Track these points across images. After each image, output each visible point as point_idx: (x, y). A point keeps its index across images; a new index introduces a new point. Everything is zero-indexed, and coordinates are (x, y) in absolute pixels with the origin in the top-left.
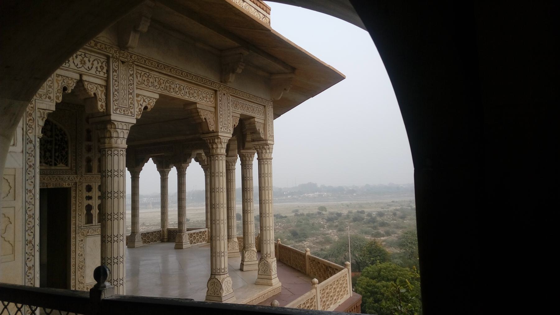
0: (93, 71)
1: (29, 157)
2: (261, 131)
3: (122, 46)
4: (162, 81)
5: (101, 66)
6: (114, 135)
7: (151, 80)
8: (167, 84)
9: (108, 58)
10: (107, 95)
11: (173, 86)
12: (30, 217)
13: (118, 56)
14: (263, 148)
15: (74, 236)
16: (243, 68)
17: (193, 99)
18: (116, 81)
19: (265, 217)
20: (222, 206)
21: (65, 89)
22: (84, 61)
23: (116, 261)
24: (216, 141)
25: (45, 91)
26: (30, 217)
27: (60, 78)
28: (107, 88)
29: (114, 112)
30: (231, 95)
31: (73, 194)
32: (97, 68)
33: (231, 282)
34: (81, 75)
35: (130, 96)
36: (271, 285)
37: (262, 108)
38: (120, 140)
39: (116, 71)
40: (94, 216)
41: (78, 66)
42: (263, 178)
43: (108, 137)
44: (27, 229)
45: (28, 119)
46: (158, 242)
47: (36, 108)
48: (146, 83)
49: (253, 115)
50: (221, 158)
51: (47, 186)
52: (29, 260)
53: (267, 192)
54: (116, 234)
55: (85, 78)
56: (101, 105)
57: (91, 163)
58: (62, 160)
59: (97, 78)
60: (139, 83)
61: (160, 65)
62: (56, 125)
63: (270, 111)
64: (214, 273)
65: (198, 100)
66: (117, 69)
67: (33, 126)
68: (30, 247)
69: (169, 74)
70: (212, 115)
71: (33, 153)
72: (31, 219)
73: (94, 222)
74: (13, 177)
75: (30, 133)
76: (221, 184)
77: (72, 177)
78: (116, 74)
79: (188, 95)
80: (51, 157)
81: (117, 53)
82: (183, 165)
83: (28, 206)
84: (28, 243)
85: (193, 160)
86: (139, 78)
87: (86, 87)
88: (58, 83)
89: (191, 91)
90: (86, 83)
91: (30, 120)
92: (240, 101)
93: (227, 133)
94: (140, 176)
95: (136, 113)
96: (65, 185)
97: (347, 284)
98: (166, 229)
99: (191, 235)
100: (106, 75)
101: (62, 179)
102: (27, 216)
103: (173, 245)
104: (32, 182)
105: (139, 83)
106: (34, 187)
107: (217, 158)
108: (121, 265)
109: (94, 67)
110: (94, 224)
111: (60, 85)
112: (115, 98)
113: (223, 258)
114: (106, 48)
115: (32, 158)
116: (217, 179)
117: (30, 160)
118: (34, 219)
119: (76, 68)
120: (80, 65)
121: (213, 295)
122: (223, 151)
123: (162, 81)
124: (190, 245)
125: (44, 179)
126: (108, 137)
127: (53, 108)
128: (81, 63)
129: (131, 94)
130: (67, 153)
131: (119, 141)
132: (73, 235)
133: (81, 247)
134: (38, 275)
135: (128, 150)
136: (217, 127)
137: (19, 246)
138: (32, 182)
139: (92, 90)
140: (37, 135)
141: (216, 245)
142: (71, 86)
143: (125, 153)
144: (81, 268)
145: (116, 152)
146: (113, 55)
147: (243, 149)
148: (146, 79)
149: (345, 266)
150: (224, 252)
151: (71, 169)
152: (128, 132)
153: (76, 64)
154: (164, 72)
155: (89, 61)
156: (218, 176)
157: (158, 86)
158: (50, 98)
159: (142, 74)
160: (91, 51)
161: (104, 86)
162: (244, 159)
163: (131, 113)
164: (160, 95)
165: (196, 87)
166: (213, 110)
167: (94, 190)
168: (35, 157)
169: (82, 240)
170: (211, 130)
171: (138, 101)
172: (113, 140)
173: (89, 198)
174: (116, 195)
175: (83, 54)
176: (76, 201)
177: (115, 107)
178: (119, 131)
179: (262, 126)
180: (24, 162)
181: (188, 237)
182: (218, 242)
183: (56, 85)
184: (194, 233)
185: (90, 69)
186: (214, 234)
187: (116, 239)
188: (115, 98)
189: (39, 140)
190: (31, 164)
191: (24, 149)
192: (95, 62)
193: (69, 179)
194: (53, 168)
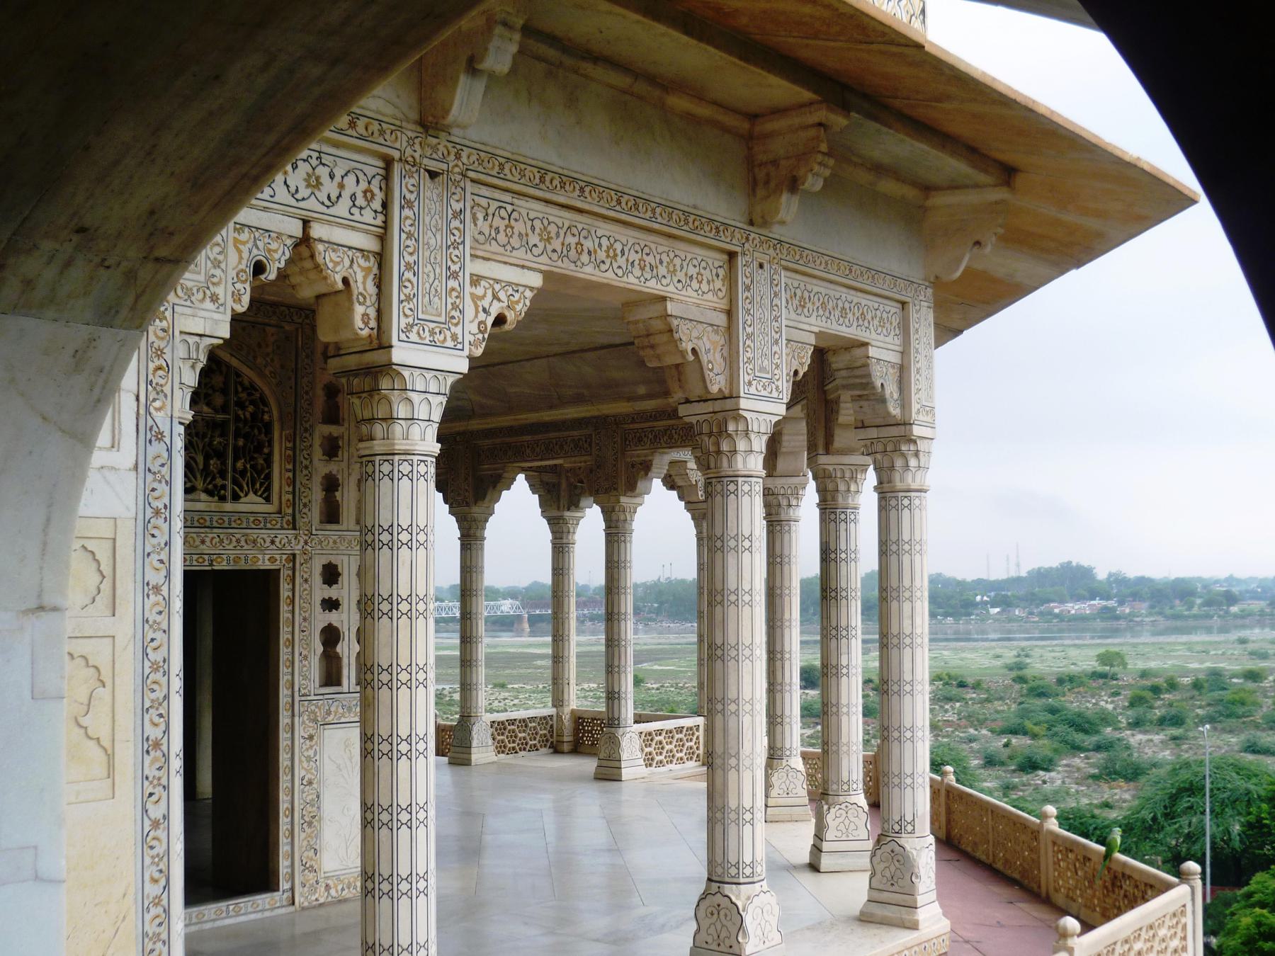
0: (342, 208)
1: (155, 485)
2: (891, 390)
3: (430, 122)
4: (553, 229)
5: (365, 192)
6: (401, 411)
7: (519, 227)
8: (572, 240)
9: (388, 163)
10: (381, 283)
11: (588, 244)
12: (155, 667)
13: (417, 155)
14: (897, 450)
15: (288, 721)
16: (827, 173)
17: (653, 287)
18: (410, 236)
19: (899, 693)
20: (747, 653)
21: (259, 268)
22: (318, 178)
23: (404, 817)
24: (731, 427)
25: (202, 278)
26: (155, 667)
27: (245, 236)
28: (382, 258)
29: (403, 337)
30: (786, 269)
31: (285, 591)
32: (353, 197)
33: (776, 909)
34: (306, 223)
35: (452, 283)
36: (914, 926)
37: (894, 308)
38: (418, 430)
39: (410, 204)
40: (345, 661)
41: (299, 196)
42: (894, 558)
43: (384, 419)
44: (147, 705)
45: (152, 366)
46: (543, 750)
47: (177, 333)
48: (502, 238)
49: (862, 335)
50: (746, 488)
51: (211, 565)
52: (154, 798)
53: (906, 607)
54: (404, 732)
55: (317, 231)
56: (365, 315)
57: (338, 494)
58: (253, 485)
59: (353, 228)
60: (481, 238)
61: (548, 178)
62: (238, 375)
63: (923, 320)
64: (720, 877)
65: (671, 288)
66: (412, 197)
67: (167, 389)
68: (155, 760)
69: (579, 204)
70: (720, 339)
71: (165, 470)
72: (158, 676)
73: (345, 681)
74: (109, 544)
75: (158, 409)
76: (746, 575)
77: (283, 536)
78: (410, 213)
79: (637, 272)
80: (223, 474)
81: (417, 147)
82: (623, 499)
83: (150, 635)
84: (151, 746)
85: (657, 484)
86: (480, 222)
87: (319, 259)
88: (240, 252)
89: (649, 259)
90: (320, 247)
91: (160, 368)
92: (817, 287)
93: (768, 399)
94: (487, 533)
95: (468, 338)
96: (264, 564)
97: (1184, 938)
98: (567, 710)
99: (648, 737)
100: (379, 222)
101: (254, 542)
102: (147, 664)
103: (589, 765)
104: (161, 561)
105: (481, 238)
106: (168, 576)
107: (732, 487)
108: (422, 831)
109: (346, 194)
110: (345, 689)
111: (245, 255)
112: (407, 291)
113: (748, 828)
114: (382, 132)
115: (162, 488)
116: (731, 560)
117: (156, 494)
118: (167, 673)
119: (293, 202)
120: (304, 192)
121: (714, 947)
122: (756, 464)
123: (553, 229)
124: (643, 771)
125: (203, 542)
126: (384, 419)
127: (225, 332)
128: (308, 186)
129: (455, 275)
130: (269, 461)
131: (416, 430)
132: (284, 719)
133: (309, 759)
134: (178, 847)
135: (440, 460)
136: (733, 378)
137: (127, 754)
138: (161, 561)
139: (336, 267)
140: (176, 414)
141: (725, 784)
142: (278, 260)
143: (432, 470)
144: (310, 824)
145: (405, 468)
146: (402, 153)
147: (828, 452)
148: (502, 224)
149: (1182, 876)
150: (752, 810)
151: (279, 512)
152: (444, 400)
153: (293, 189)
154: (562, 200)
155: (332, 176)
156: (736, 549)
157: (541, 246)
158: (214, 298)
159: (491, 211)
160: (337, 145)
161: (376, 254)
162: (830, 487)
163: (454, 337)
164: (547, 276)
165: (664, 245)
166: (721, 320)
167: (344, 579)
168: (169, 483)
169: (311, 738)
170: (714, 389)
171: (475, 298)
172: (398, 429)
173: (331, 605)
174: (404, 607)
175: (315, 155)
176: (293, 612)
177: (404, 321)
178: (415, 397)
179: (893, 374)
180: (141, 498)
181: (637, 743)
182: (732, 775)
183: (233, 256)
184: (659, 732)
185: (332, 202)
186: (719, 749)
187: (404, 747)
188: (407, 291)
189: (182, 428)
190: (161, 506)
191: (141, 458)
192: (350, 180)
193: (273, 542)
194: (229, 506)
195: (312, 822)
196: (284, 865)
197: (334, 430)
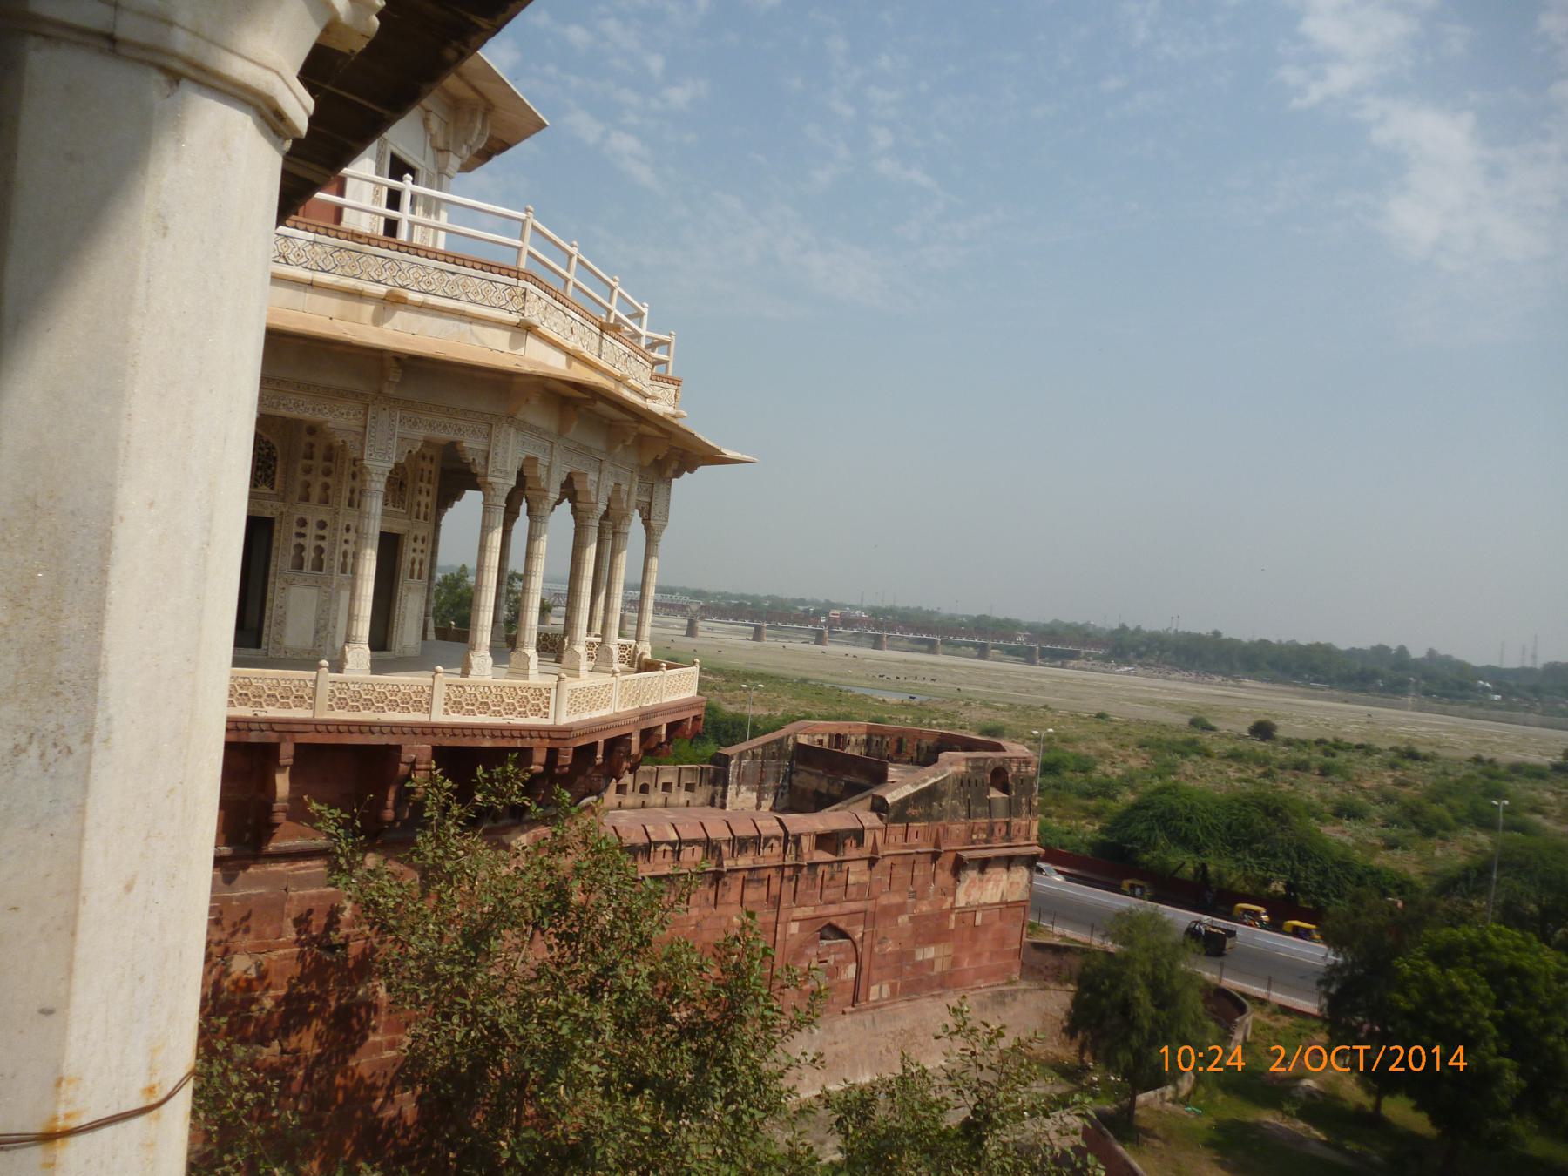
17: (319, 417)
49: (457, 437)
77: (277, 504)
96: (267, 514)
166: (361, 430)
195: (281, 623)
196: (265, 639)
197: (309, 462)
